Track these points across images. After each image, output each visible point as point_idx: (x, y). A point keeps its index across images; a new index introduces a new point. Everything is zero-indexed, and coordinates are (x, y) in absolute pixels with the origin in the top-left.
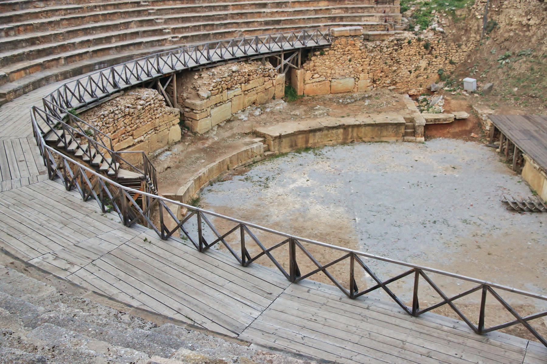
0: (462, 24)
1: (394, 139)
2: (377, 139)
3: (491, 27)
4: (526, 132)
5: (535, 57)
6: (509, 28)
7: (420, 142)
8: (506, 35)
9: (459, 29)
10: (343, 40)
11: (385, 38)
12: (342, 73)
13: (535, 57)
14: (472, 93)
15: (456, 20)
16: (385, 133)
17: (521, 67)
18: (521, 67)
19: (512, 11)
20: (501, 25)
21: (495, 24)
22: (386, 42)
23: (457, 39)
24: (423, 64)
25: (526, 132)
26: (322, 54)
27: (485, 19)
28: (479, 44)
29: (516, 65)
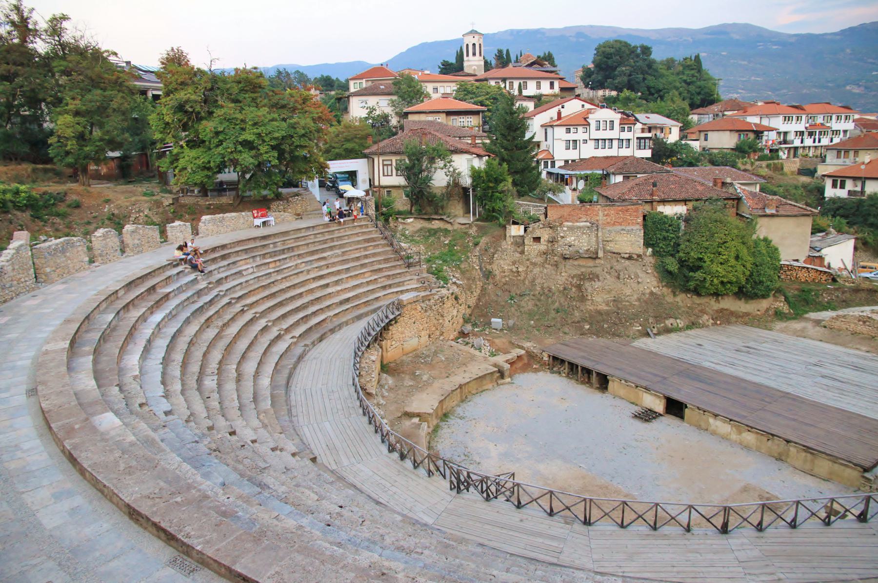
0: (468, 275)
1: (490, 386)
2: (480, 389)
3: (488, 275)
4: (583, 357)
5: (534, 295)
6: (503, 274)
7: (509, 383)
8: (503, 280)
9: (468, 279)
10: (410, 306)
11: (431, 297)
12: (410, 335)
13: (534, 295)
14: (502, 330)
15: (463, 273)
16: (484, 382)
17: (528, 304)
18: (528, 304)
19: (502, 262)
20: (497, 273)
21: (490, 272)
22: (432, 301)
23: (470, 288)
24: (455, 313)
25: (583, 357)
26: (396, 322)
27: (481, 269)
28: (483, 289)
29: (523, 303)
